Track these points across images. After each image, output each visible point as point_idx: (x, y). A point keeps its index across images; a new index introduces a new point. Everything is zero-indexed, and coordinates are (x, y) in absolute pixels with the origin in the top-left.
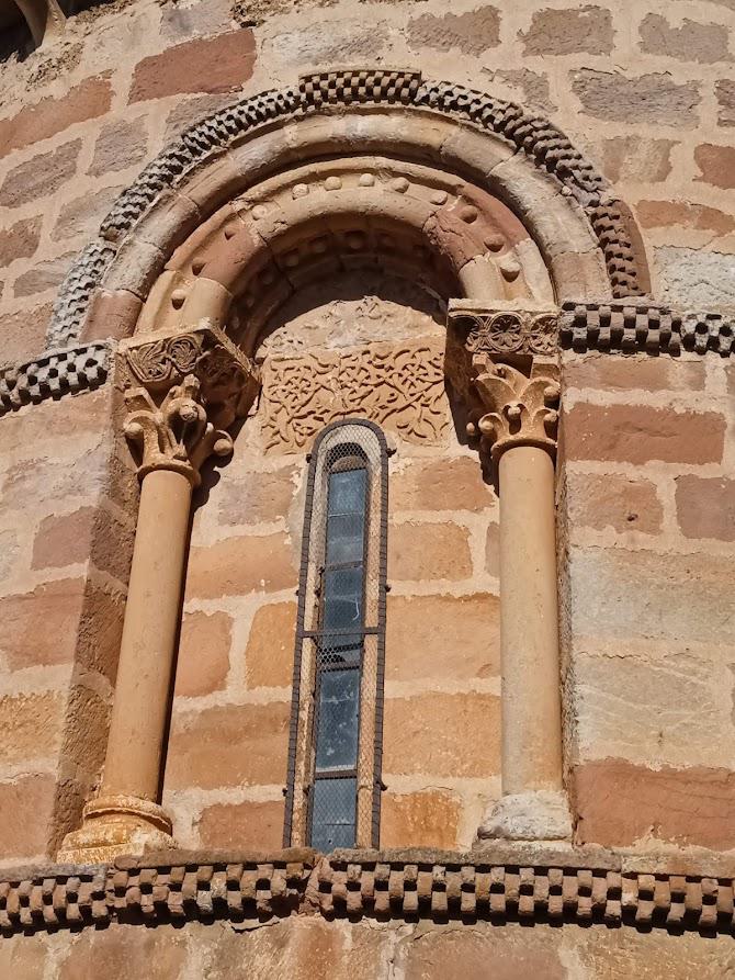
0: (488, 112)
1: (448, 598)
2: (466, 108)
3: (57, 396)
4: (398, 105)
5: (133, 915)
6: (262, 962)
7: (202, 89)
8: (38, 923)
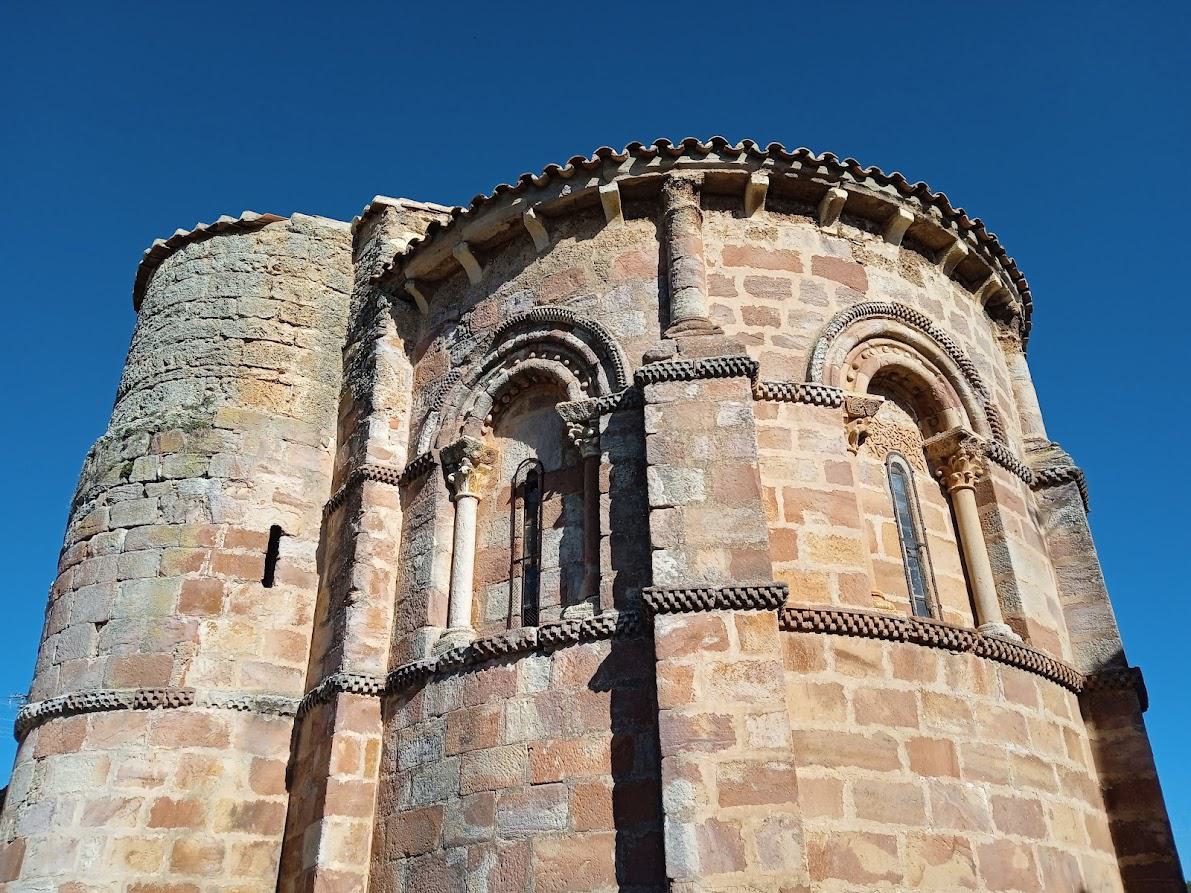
0: (952, 349)
1: (942, 539)
2: (945, 344)
3: (817, 404)
4: (922, 330)
5: (919, 641)
6: (962, 667)
7: (847, 284)
8: (881, 636)
